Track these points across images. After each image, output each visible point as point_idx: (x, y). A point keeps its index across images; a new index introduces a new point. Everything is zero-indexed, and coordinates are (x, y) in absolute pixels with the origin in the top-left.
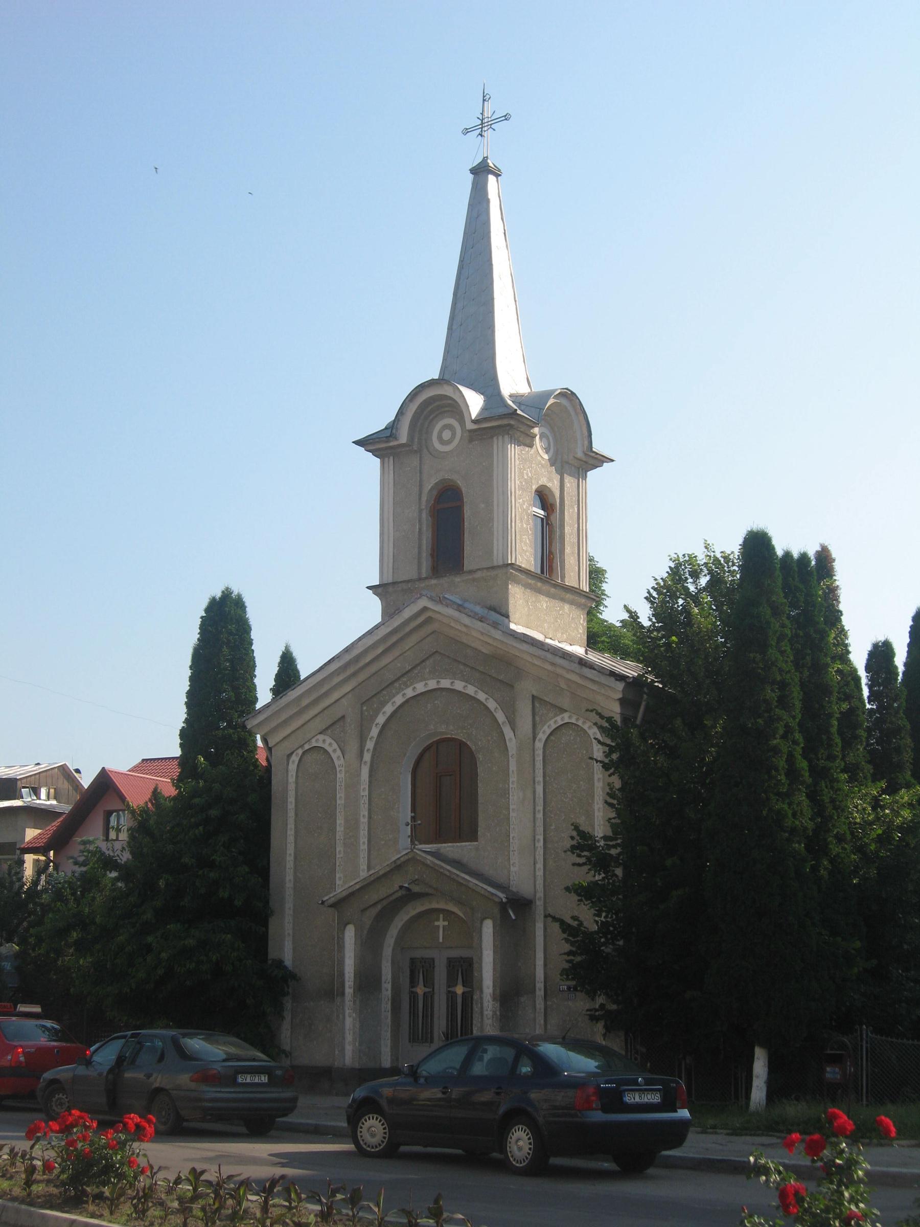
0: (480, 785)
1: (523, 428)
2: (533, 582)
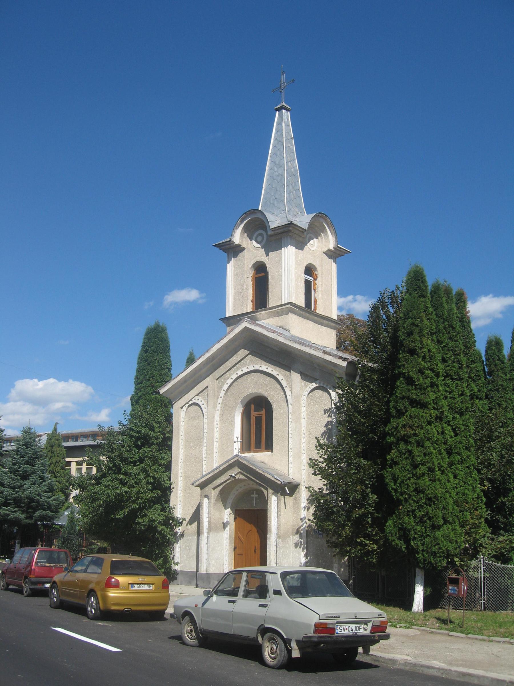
0: (274, 421)
1: (297, 232)
2: (304, 313)
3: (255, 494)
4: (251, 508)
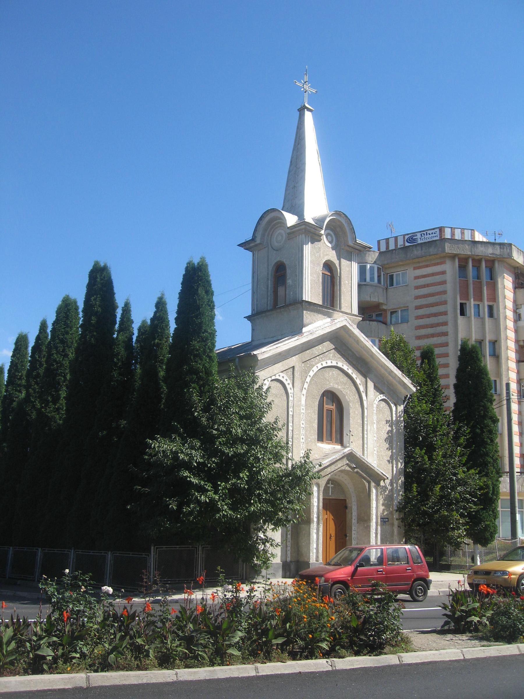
3: (330, 483)
4: (327, 498)
